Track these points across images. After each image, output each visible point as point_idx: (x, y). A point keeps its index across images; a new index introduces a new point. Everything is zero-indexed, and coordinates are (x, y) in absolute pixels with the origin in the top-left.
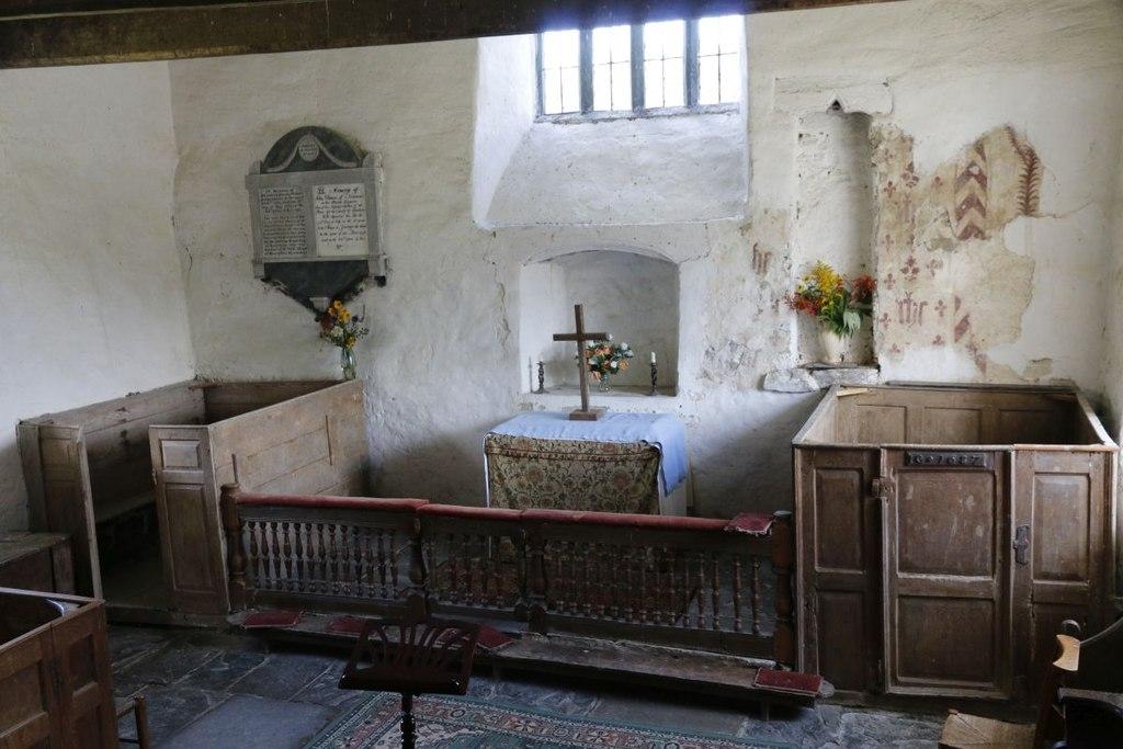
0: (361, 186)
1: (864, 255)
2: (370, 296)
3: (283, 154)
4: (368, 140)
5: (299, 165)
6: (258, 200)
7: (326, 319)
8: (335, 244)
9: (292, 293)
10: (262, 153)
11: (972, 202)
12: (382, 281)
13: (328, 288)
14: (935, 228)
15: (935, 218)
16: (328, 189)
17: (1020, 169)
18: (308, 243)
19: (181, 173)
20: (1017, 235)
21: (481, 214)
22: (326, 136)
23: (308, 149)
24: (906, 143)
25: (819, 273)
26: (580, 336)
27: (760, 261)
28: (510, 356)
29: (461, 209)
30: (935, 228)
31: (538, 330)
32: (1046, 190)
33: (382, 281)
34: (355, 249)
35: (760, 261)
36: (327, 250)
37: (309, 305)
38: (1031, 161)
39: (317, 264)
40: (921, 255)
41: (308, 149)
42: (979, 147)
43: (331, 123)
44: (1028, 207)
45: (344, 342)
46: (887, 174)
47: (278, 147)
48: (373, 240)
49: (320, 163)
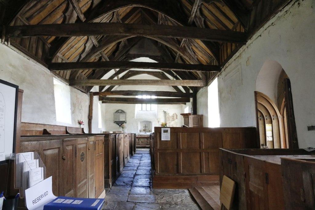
0: (125, 115)
1: (166, 122)
2: (124, 124)
3: (117, 111)
4: (125, 111)
5: (119, 113)
6: (114, 116)
7: (120, 126)
8: (122, 119)
9: (117, 124)
10: (116, 111)
11: (173, 118)
12: (126, 123)
13: (120, 124)
14: (171, 120)
15: (171, 119)
16: (122, 115)
17: (176, 116)
18: (119, 119)
19: (106, 113)
20: (176, 120)
21: (135, 118)
22: (122, 111)
23: (120, 111)
24: (169, 114)
25: (162, 123)
26: (145, 127)
27: (159, 122)
28: (138, 129)
29: (134, 117)
30: (171, 120)
31: (140, 127)
32: (178, 117)
33: (126, 123)
34: (124, 120)
35: (159, 122)
36: (121, 120)
37: (118, 125)
38: (177, 115)
39: (120, 121)
40: (170, 122)
41: (120, 111)
42: (174, 114)
43: (122, 109)
44: (177, 118)
45: (123, 128)
46: (167, 116)
47: (117, 111)
48: (126, 119)
49: (121, 113)
